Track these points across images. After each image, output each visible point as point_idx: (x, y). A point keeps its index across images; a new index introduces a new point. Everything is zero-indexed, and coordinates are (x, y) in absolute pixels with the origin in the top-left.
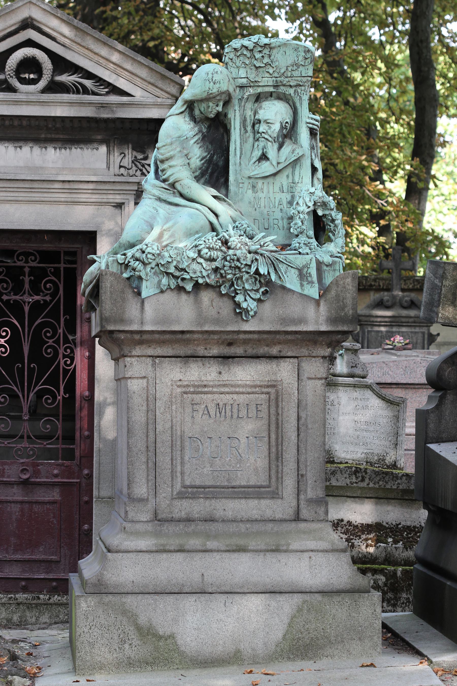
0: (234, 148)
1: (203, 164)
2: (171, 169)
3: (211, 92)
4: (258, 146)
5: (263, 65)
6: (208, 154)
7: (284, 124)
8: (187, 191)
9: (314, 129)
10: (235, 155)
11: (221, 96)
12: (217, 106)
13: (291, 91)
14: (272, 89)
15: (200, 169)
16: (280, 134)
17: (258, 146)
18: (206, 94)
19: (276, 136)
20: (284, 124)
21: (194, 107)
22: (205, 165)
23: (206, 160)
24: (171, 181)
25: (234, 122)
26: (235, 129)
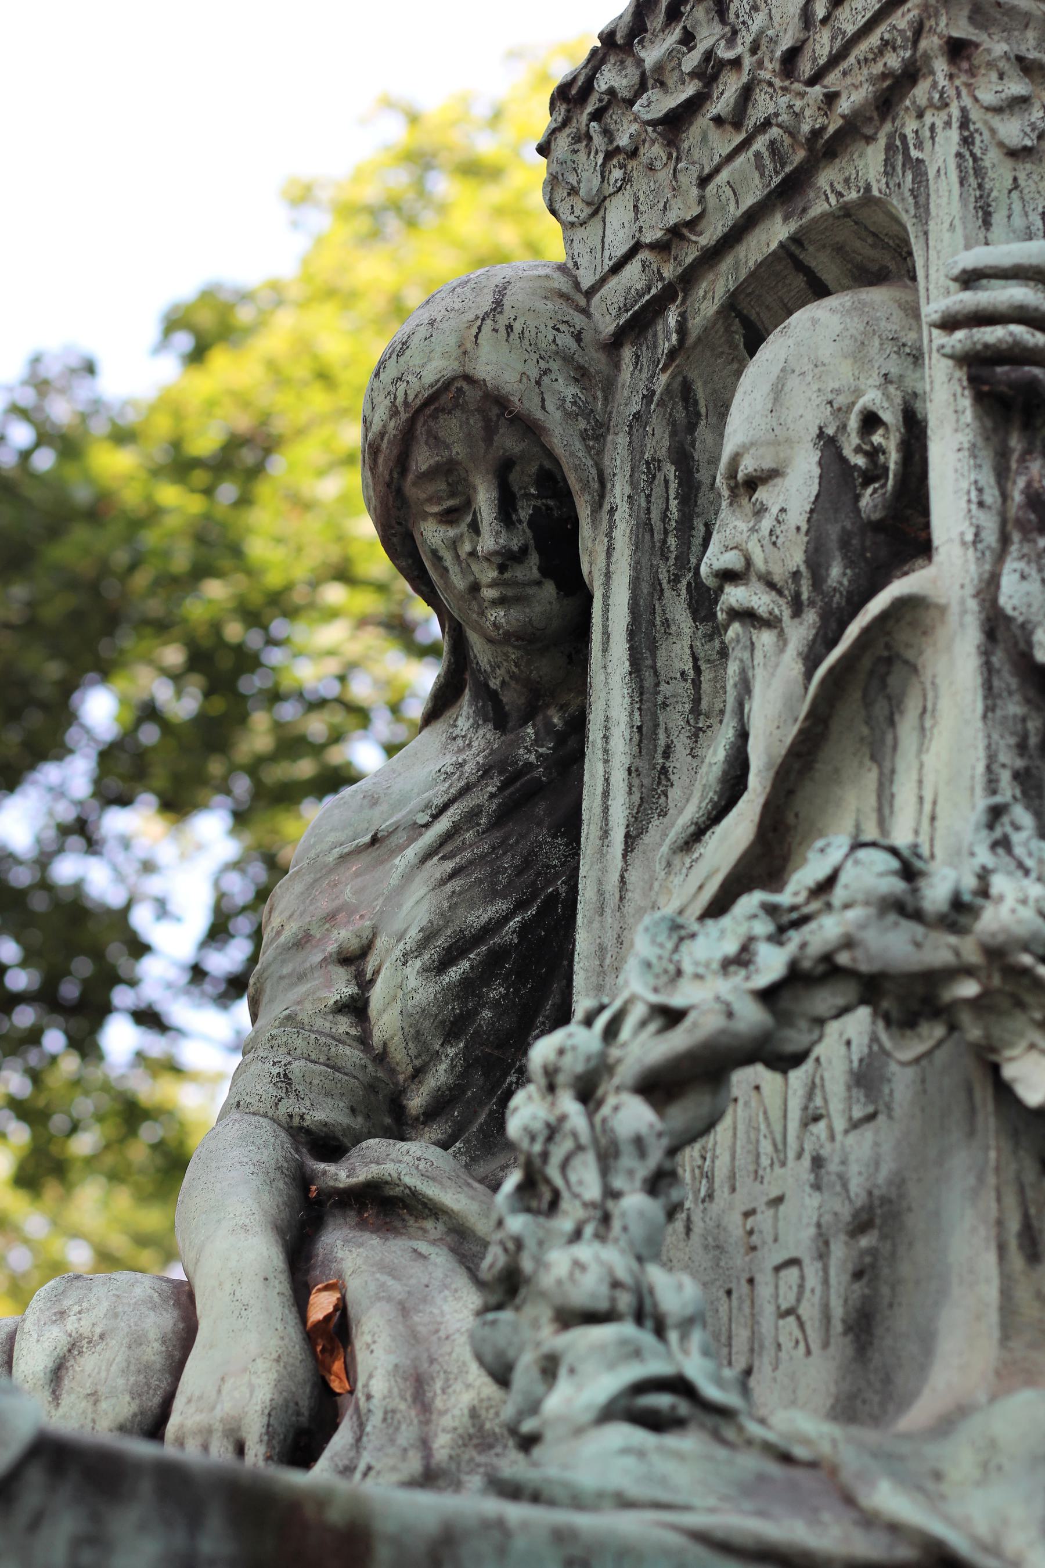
0: (599, 790)
1: (468, 986)
5: (690, 89)
6: (520, 906)
7: (850, 443)
9: (1015, 355)
11: (436, 441)
12: (475, 528)
14: (776, 231)
15: (452, 1030)
16: (833, 532)
19: (796, 558)
20: (850, 443)
22: (496, 992)
23: (496, 958)
25: (606, 597)
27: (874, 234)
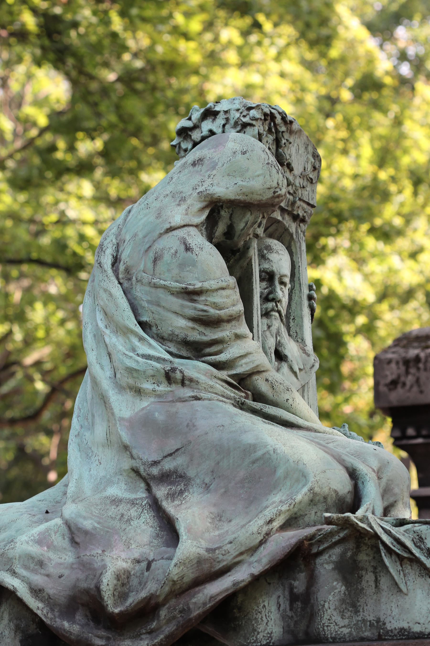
0: (257, 323)
2: (239, 342)
3: (279, 192)
4: (269, 327)
8: (286, 396)
10: (258, 337)
13: (293, 227)
17: (269, 327)
18: (269, 194)
21: (220, 217)
24: (242, 368)
25: (255, 268)
26: (256, 281)
27: (281, 237)
